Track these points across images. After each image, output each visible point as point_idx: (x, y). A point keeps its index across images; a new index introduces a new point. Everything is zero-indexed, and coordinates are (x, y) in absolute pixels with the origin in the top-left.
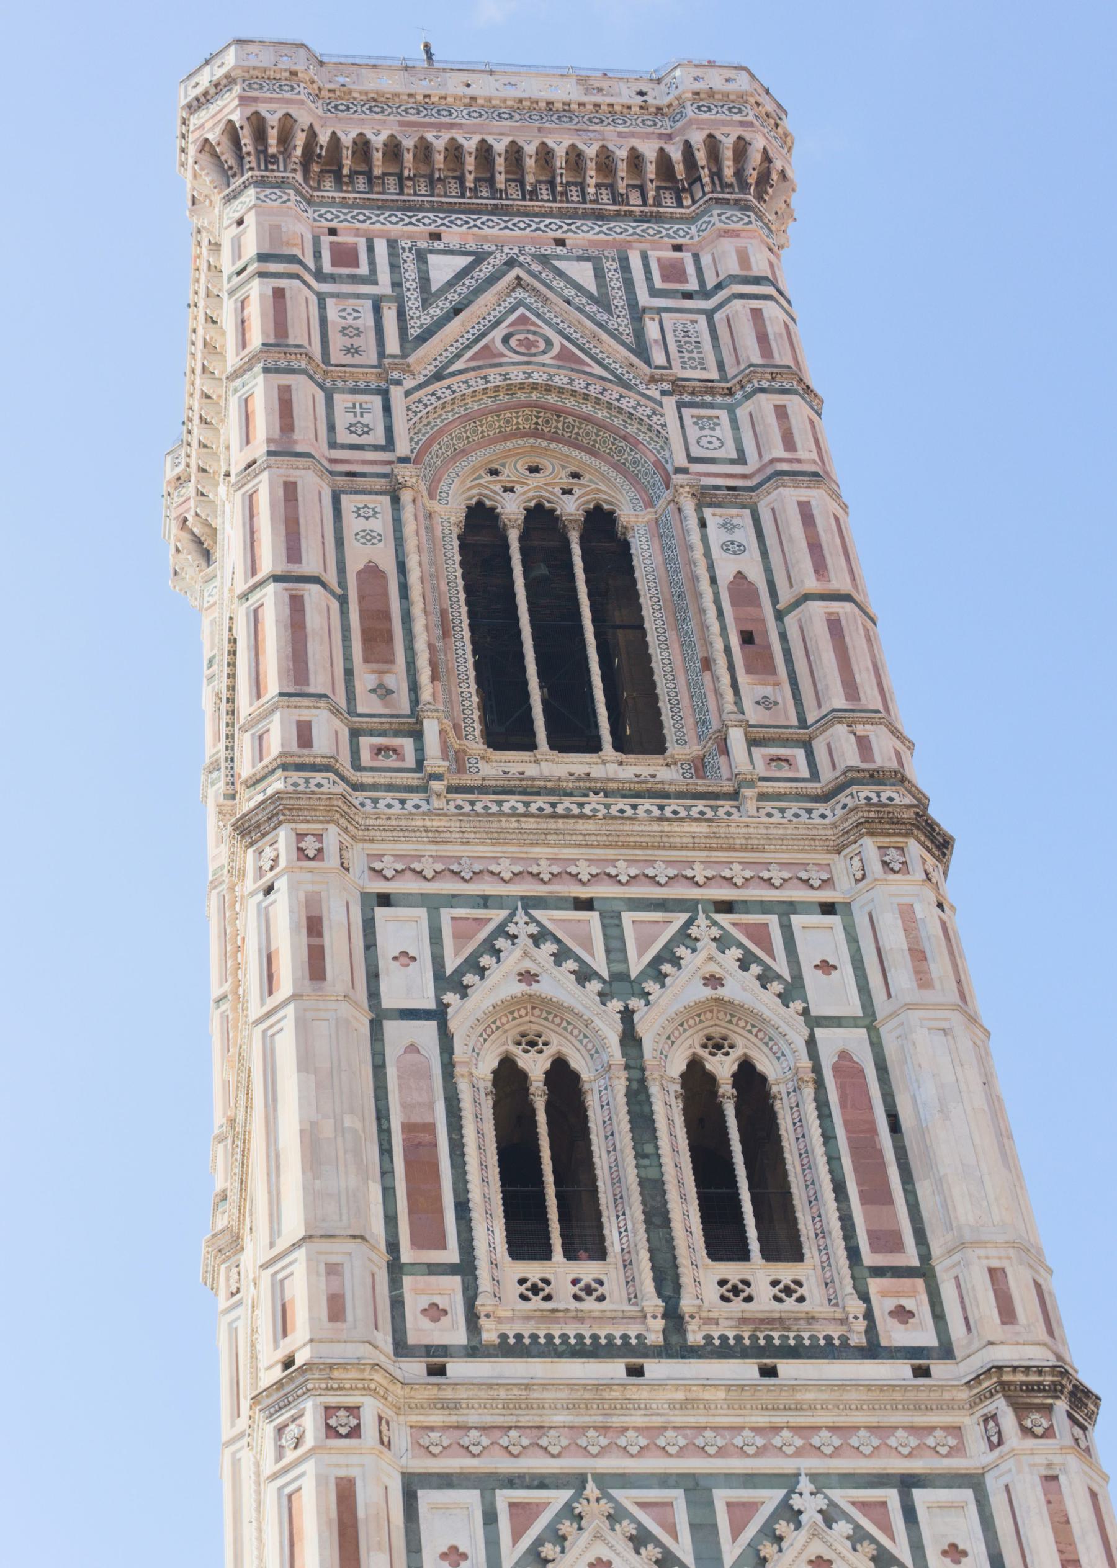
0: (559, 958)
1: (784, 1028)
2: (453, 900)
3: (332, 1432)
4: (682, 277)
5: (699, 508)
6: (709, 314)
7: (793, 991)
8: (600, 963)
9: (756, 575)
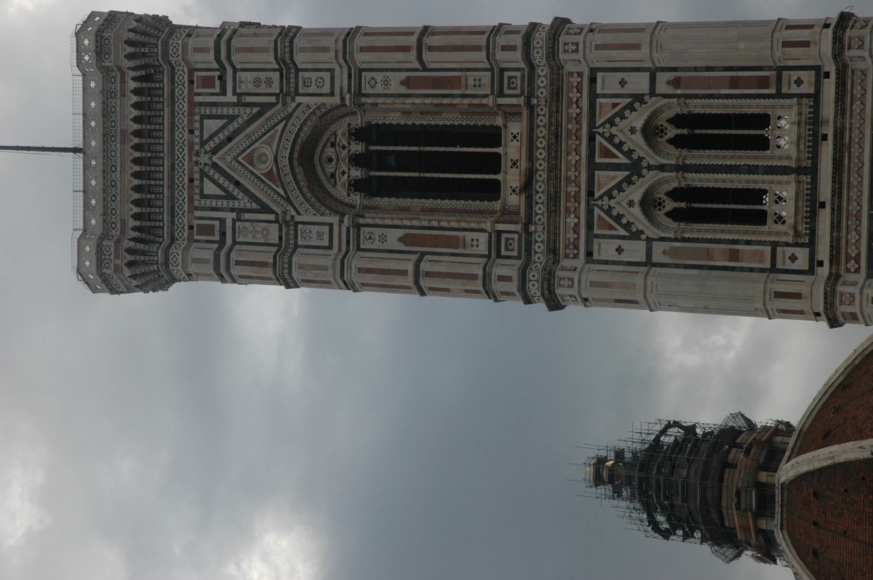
0: (621, 190)
1: (658, 105)
2: (590, 226)
3: (852, 303)
4: (213, 78)
5: (365, 95)
6: (235, 70)
7: (639, 98)
8: (622, 174)
9: (403, 75)
